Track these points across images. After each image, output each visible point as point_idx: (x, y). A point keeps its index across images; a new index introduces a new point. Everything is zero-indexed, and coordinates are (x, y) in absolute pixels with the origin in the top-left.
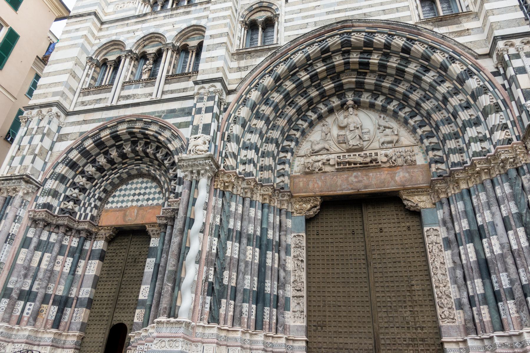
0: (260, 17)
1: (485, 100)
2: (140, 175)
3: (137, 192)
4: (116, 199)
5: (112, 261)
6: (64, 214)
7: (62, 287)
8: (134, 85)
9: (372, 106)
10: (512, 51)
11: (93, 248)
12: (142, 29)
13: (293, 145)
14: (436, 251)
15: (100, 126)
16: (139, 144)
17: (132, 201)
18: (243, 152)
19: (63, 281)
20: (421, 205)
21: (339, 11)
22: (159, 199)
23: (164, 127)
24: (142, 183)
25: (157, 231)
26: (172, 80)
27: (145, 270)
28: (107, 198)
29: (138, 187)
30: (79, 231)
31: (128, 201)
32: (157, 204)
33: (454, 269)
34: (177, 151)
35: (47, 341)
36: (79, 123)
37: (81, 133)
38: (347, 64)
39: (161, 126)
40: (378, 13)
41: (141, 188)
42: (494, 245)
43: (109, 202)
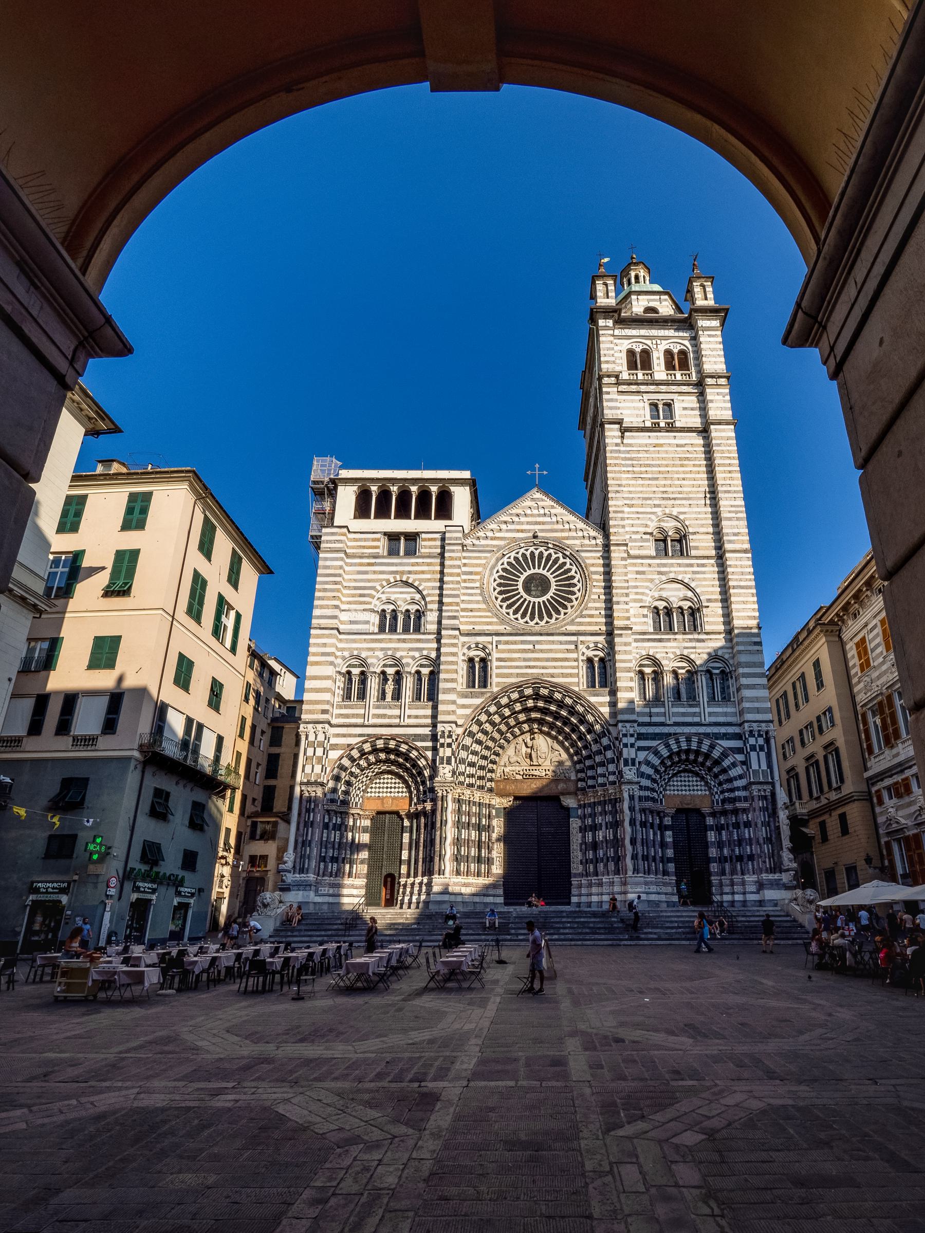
0: (477, 654)
1: (609, 754)
3: (389, 785)
4: (373, 790)
9: (548, 734)
10: (624, 732)
12: (382, 649)
13: (497, 759)
14: (575, 832)
18: (468, 768)
20: (571, 806)
21: (533, 667)
28: (366, 789)
33: (581, 844)
38: (535, 707)
40: (558, 676)
42: (600, 835)
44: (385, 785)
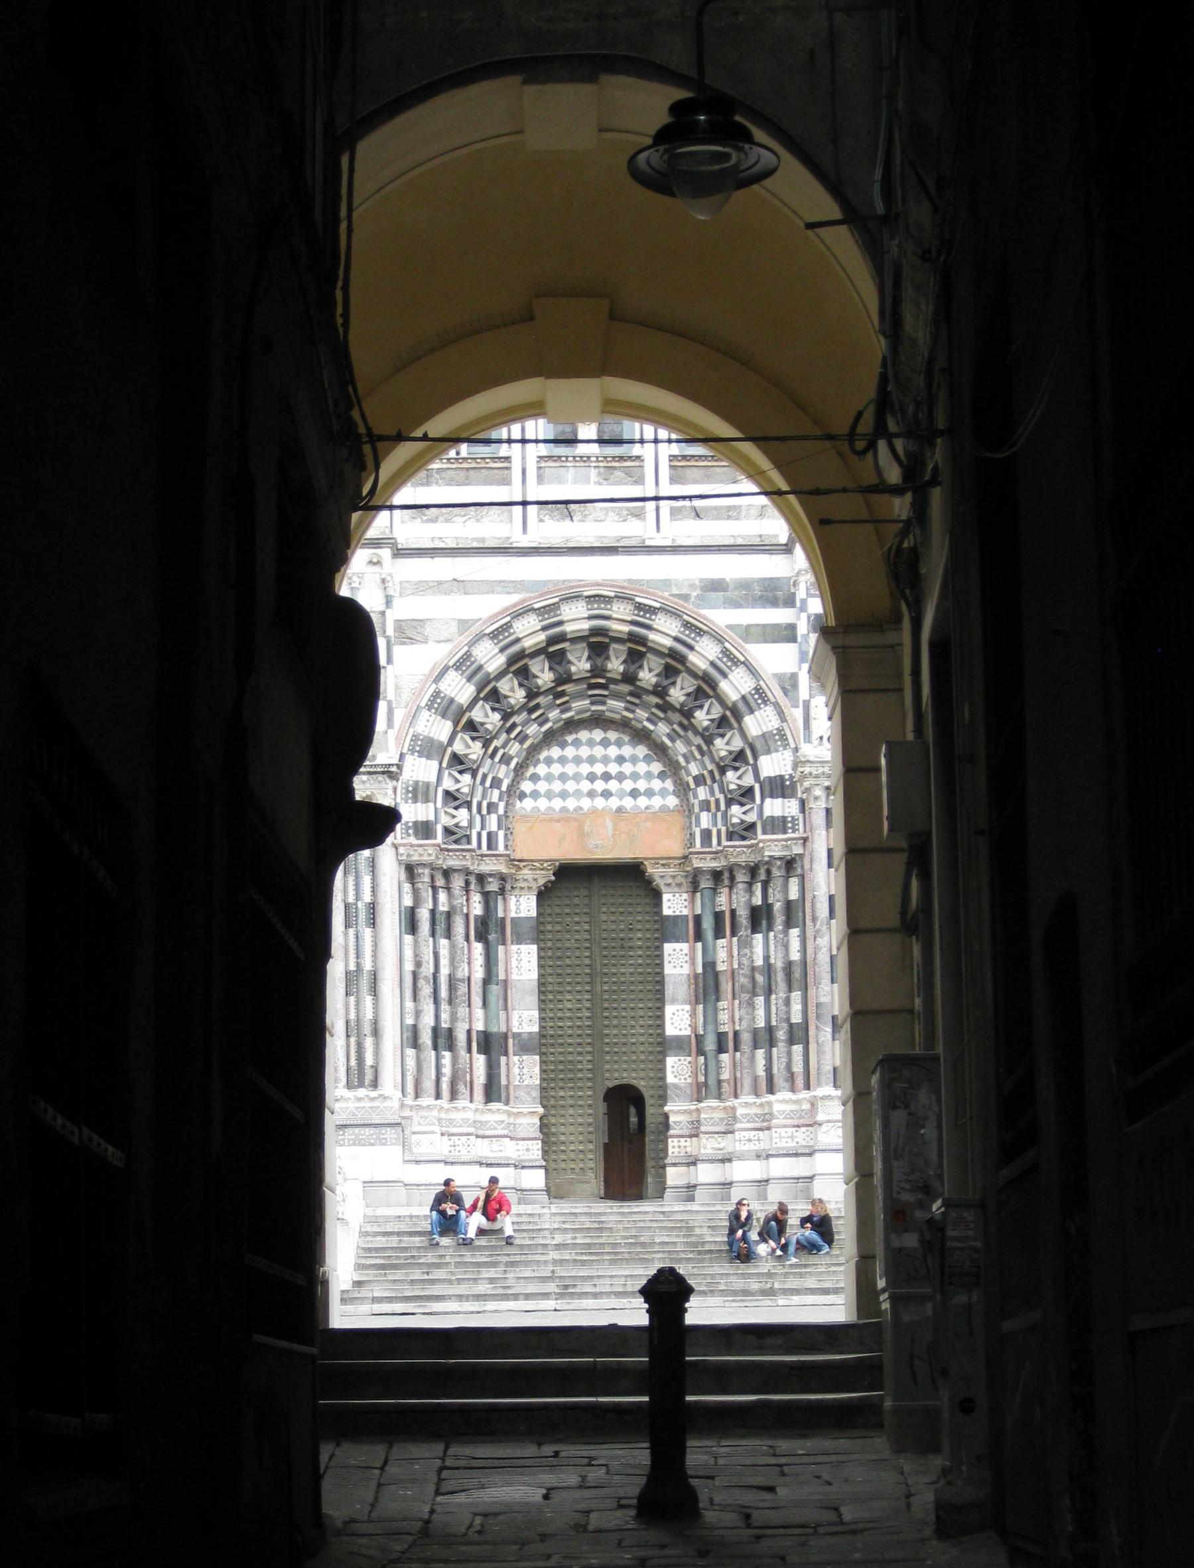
2: (597, 721)
3: (599, 769)
4: (542, 786)
5: (559, 945)
6: (456, 842)
7: (479, 1013)
8: (572, 470)
11: (513, 915)
15: (515, 605)
16: (611, 653)
17: (591, 794)
19: (477, 1000)
22: (663, 793)
23: (700, 630)
24: (605, 743)
25: (674, 877)
26: (688, 472)
27: (667, 971)
29: (599, 756)
30: (481, 878)
31: (578, 794)
32: (664, 809)
34: (749, 704)
35: (495, 1128)
36: (437, 587)
37: (464, 625)
39: (688, 623)
41: (605, 760)
43: (522, 796)
44: (585, 769)
